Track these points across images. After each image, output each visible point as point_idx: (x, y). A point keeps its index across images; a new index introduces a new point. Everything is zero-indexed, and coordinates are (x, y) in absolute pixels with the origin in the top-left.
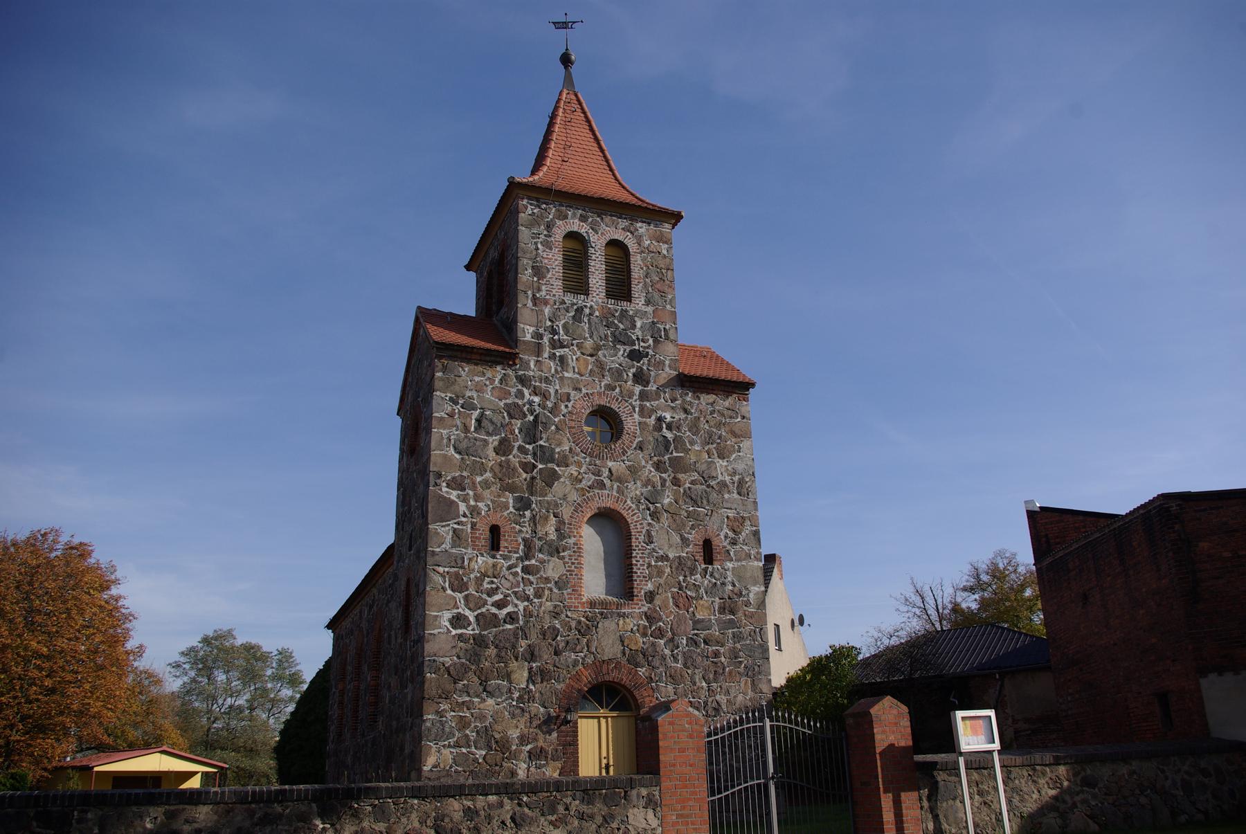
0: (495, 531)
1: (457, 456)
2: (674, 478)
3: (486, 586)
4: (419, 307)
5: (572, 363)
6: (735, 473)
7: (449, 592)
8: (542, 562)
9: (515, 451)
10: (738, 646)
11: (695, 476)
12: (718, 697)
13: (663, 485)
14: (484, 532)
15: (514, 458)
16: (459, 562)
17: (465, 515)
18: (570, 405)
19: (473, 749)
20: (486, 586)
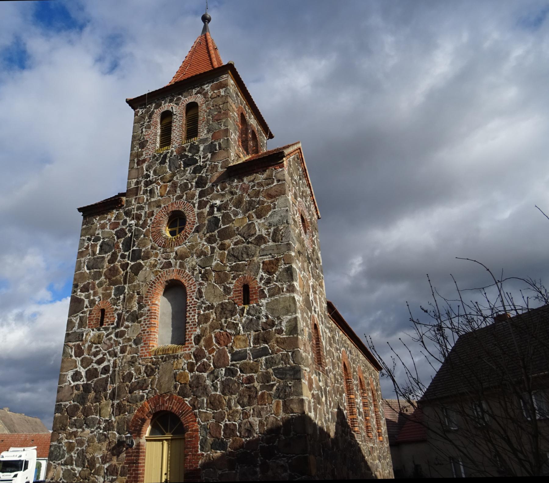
0: (103, 311)
1: (88, 271)
2: (222, 244)
3: (93, 350)
6: (270, 225)
7: (74, 358)
9: (119, 258)
10: (270, 370)
12: (251, 419)
13: (213, 252)
14: (97, 315)
16: (80, 337)
17: (87, 307)
18: (153, 218)
19: (74, 467)
20: (93, 350)
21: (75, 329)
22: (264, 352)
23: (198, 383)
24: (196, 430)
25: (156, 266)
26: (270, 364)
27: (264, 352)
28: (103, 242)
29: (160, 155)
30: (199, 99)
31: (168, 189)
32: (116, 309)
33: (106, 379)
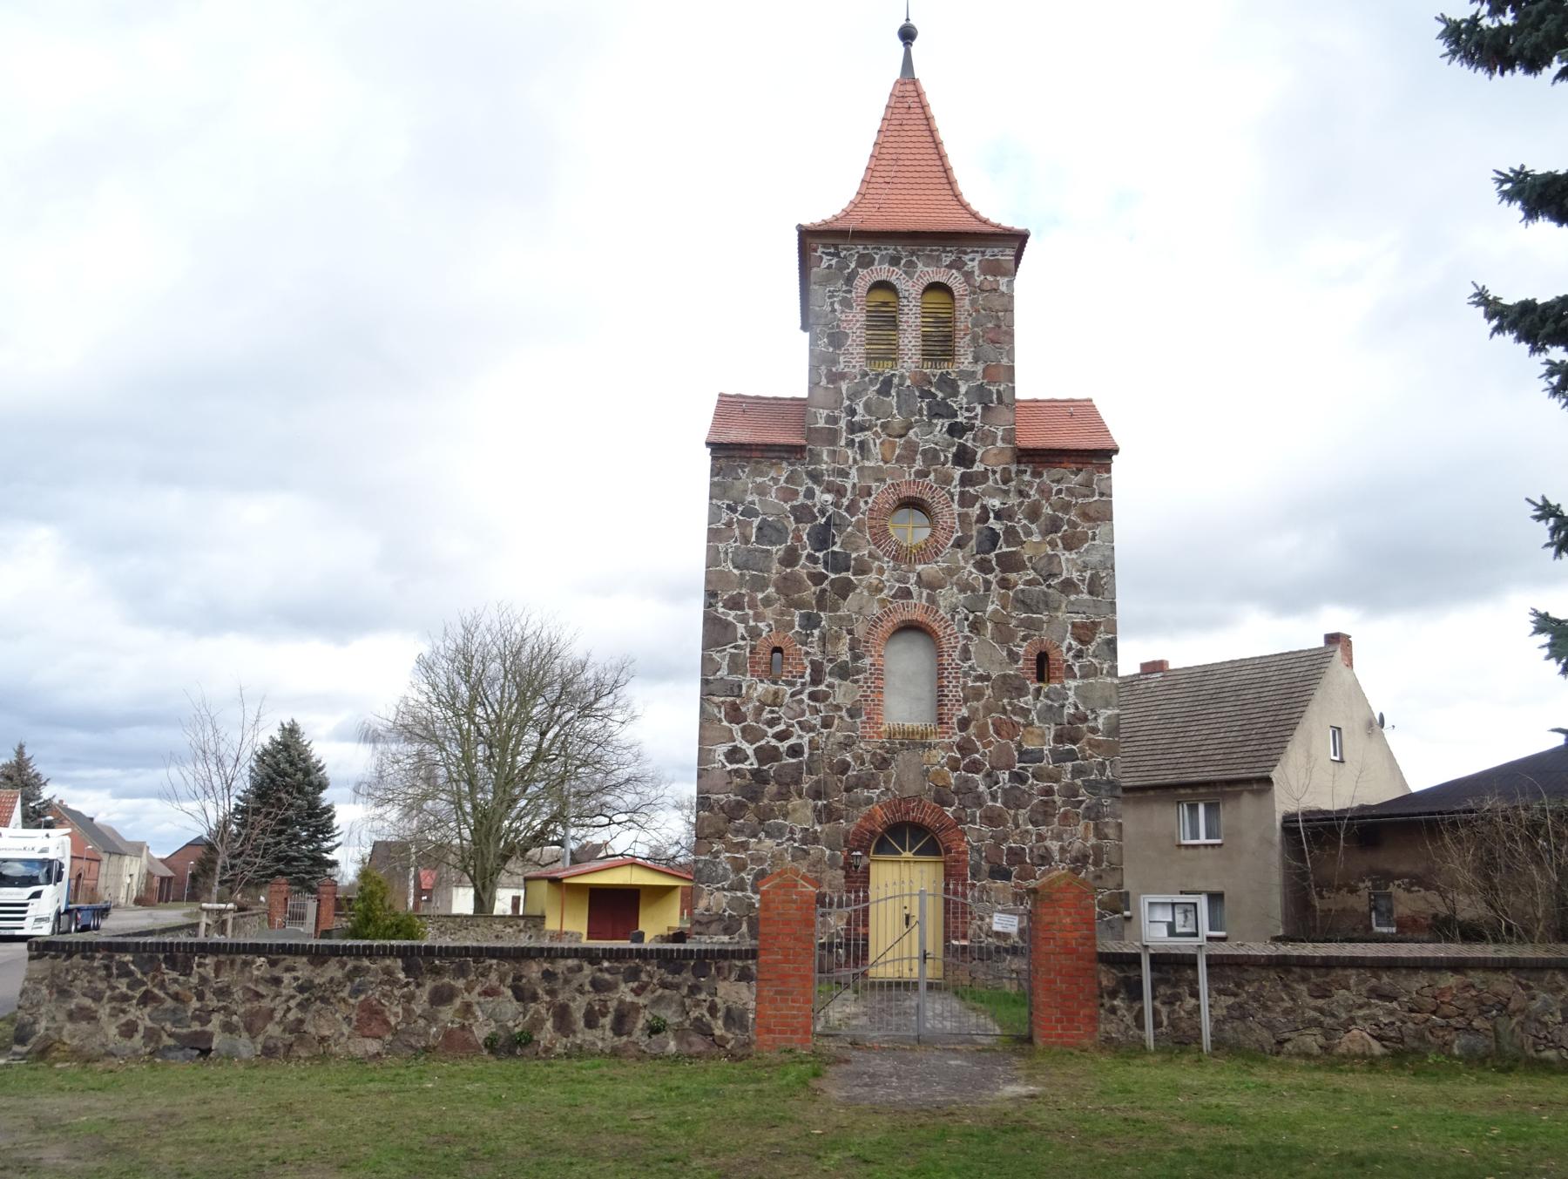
1: (736, 572)
2: (1003, 579)
3: (766, 715)
4: (721, 395)
5: (876, 450)
6: (1086, 566)
7: (725, 723)
8: (831, 686)
9: (803, 561)
10: (1078, 782)
11: (1032, 574)
12: (1048, 843)
13: (987, 589)
14: (764, 655)
15: (802, 569)
16: (736, 690)
17: (743, 638)
19: (750, 894)
20: (766, 715)
21: (723, 673)
22: (1071, 756)
23: (966, 789)
24: (965, 853)
25: (881, 590)
26: (1077, 772)
27: (1071, 756)
28: (764, 520)
29: (878, 375)
30: (955, 281)
31: (898, 451)
32: (807, 653)
33: (799, 766)
